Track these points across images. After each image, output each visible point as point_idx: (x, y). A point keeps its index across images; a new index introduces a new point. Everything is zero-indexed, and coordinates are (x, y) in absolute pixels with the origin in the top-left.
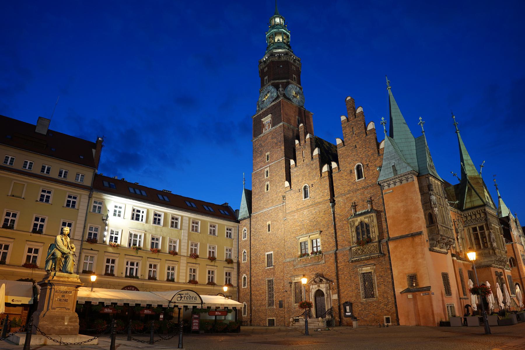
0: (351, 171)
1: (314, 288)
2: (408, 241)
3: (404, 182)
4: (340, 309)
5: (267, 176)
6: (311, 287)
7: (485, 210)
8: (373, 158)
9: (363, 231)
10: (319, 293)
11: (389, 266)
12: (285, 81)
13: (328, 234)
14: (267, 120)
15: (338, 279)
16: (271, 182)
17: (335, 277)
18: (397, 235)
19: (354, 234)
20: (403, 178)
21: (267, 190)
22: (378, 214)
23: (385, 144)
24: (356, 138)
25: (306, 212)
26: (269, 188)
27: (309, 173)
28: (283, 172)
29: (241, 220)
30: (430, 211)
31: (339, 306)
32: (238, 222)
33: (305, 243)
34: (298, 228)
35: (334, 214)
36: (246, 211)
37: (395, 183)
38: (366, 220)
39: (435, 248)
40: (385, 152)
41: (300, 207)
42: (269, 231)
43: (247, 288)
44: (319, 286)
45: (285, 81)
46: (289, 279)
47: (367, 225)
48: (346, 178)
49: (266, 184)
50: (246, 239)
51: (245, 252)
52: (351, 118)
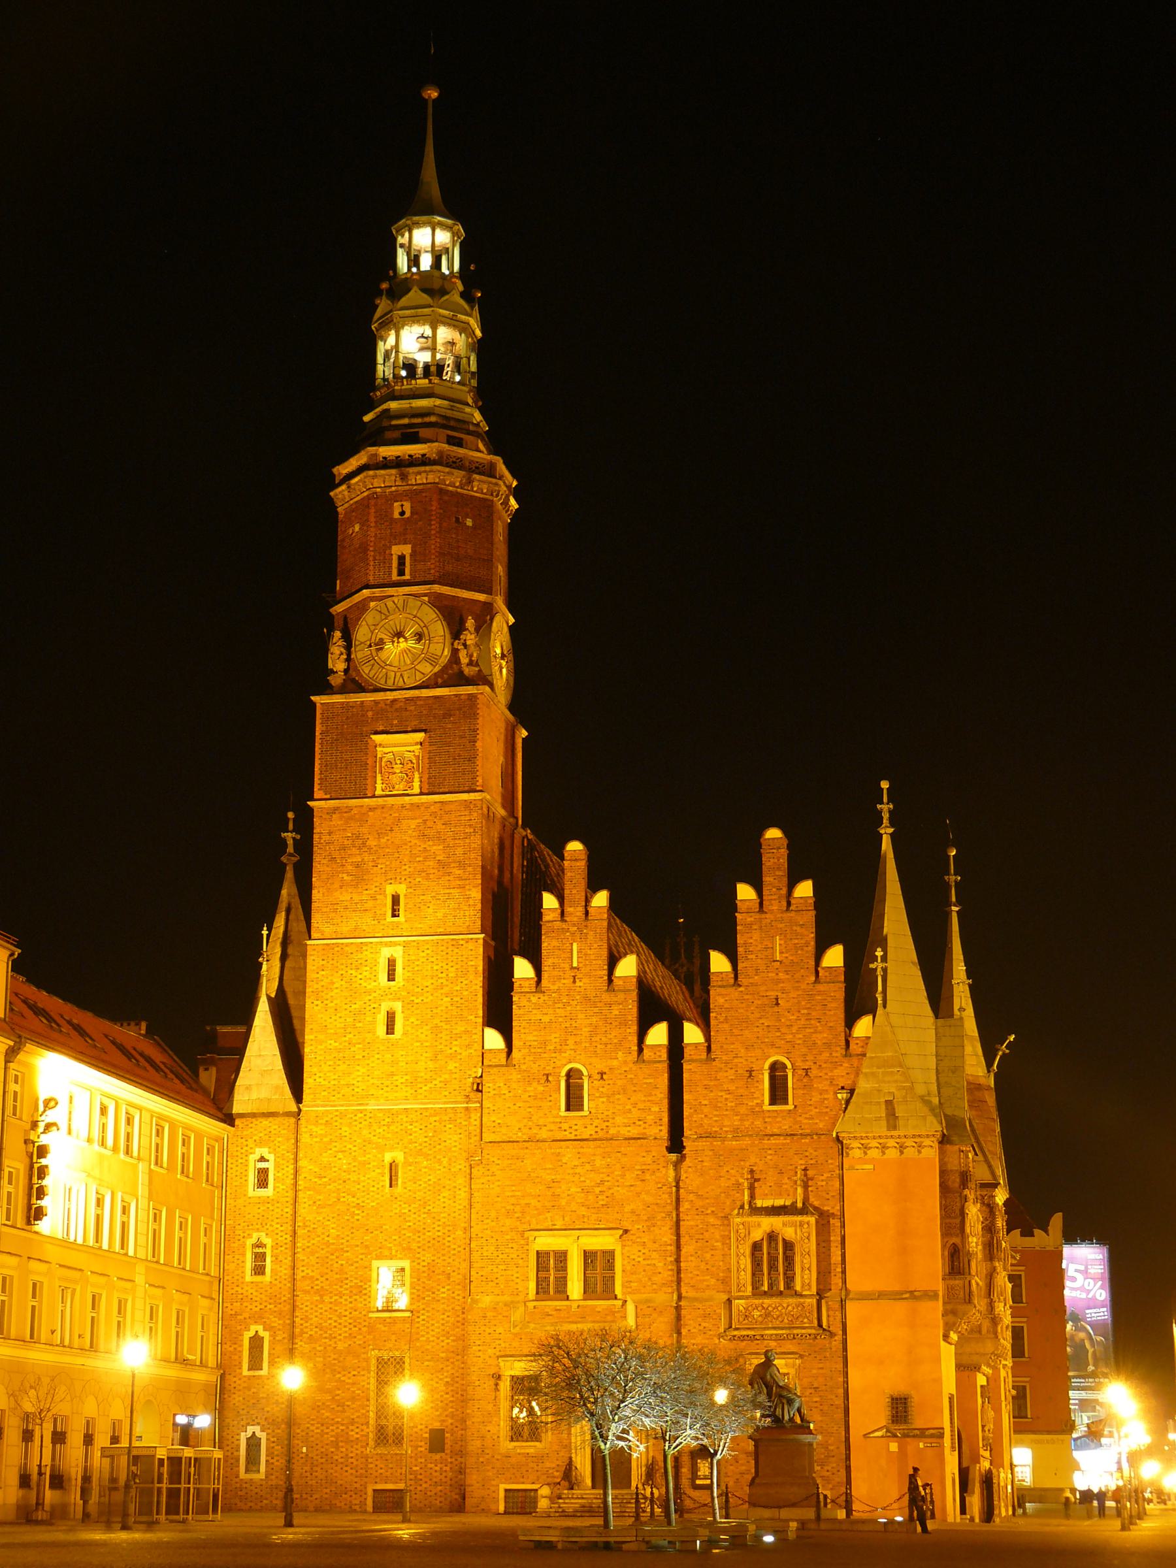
0: (750, 1071)
2: (900, 1309)
3: (910, 1152)
5: (391, 977)
8: (826, 1055)
11: (840, 1366)
12: (482, 597)
13: (650, 1245)
16: (408, 1005)
18: (868, 1286)
19: (746, 1262)
20: (909, 1142)
21: (390, 1030)
22: (824, 1219)
25: (569, 1154)
28: (474, 987)
29: (242, 1116)
30: (956, 1240)
32: (229, 1119)
33: (562, 1257)
34: (533, 1202)
35: (678, 1187)
36: (277, 1087)
37: (884, 1148)
38: (789, 1233)
41: (544, 1134)
45: (482, 597)
46: (492, 1362)
47: (789, 1246)
48: (732, 1087)
49: (385, 1007)
50: (269, 1192)
51: (259, 1245)
52: (774, 904)
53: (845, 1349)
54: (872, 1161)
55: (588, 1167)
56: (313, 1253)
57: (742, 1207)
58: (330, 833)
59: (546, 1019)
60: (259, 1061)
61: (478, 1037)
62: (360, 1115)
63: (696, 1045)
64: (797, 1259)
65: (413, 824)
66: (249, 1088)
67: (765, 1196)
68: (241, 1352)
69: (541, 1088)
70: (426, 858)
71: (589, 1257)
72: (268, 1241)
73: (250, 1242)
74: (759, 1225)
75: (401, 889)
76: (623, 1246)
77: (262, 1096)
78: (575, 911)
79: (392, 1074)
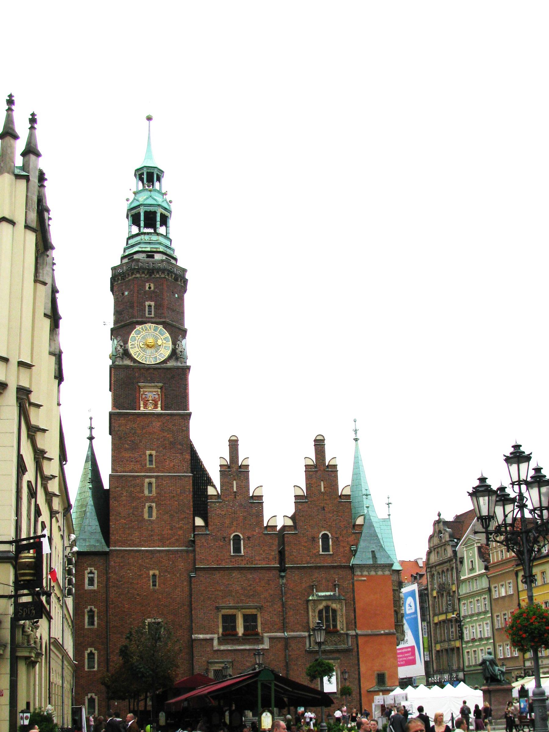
0: (314, 539)
8: (345, 532)
9: (327, 618)
21: (150, 515)
24: (325, 497)
27: (245, 518)
28: (188, 498)
34: (220, 594)
38: (334, 606)
42: (154, 585)
43: (98, 671)
47: (334, 611)
49: (147, 505)
51: (91, 611)
53: (358, 655)
54: (366, 576)
55: (244, 578)
56: (116, 616)
57: (313, 596)
58: (119, 427)
59: (223, 513)
60: (89, 528)
61: (191, 521)
62: (137, 554)
68: (84, 660)
69: (222, 543)
70: (164, 439)
71: (246, 618)
72: (96, 610)
74: (321, 603)
75: (154, 453)
76: (261, 613)
77: (92, 544)
79: (152, 536)
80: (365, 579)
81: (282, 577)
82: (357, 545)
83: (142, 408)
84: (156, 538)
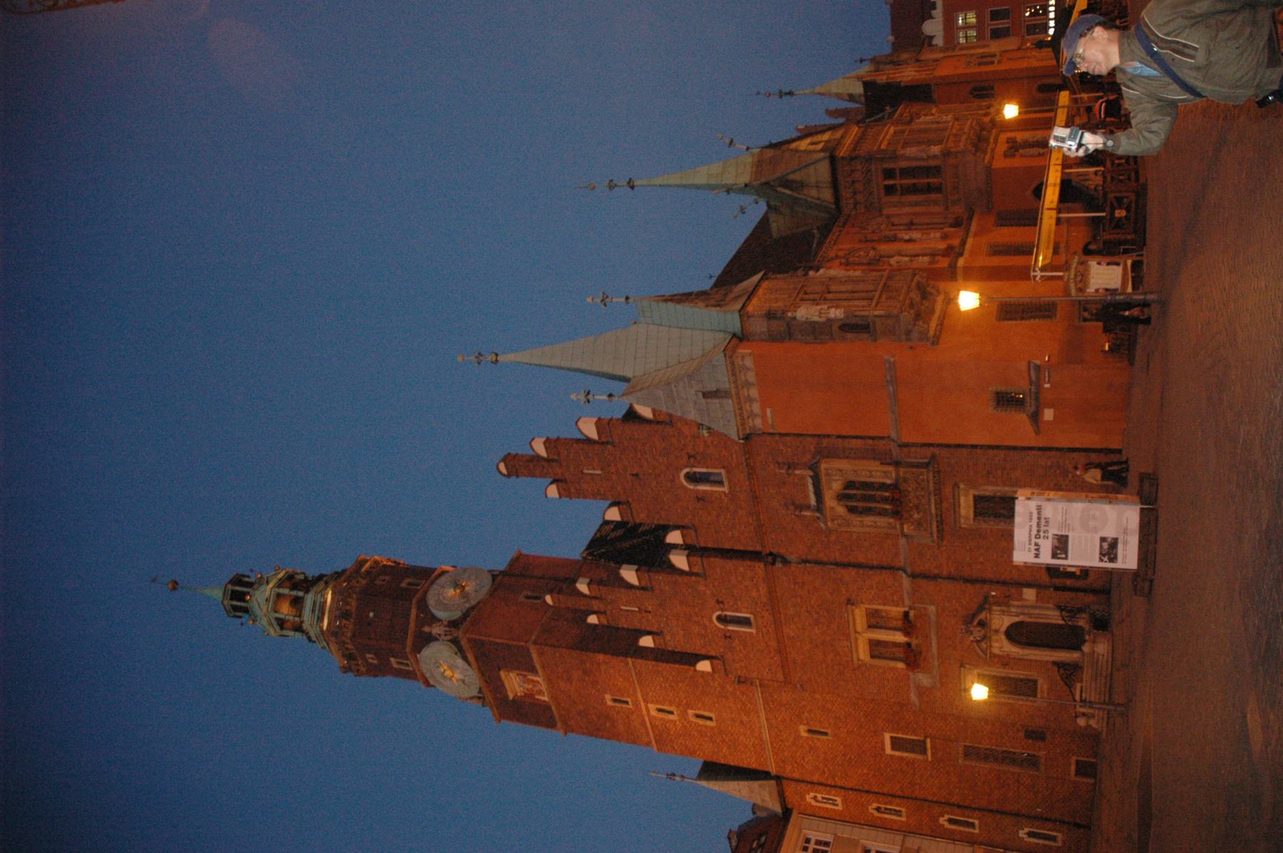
0: (701, 498)
1: (1002, 646)
4: (1064, 589)
5: (672, 713)
6: (996, 651)
7: (843, 158)
10: (1016, 634)
11: (965, 451)
14: (514, 683)
15: (984, 581)
16: (689, 706)
17: (978, 586)
19: (869, 520)
21: (710, 719)
23: (645, 405)
26: (706, 714)
28: (669, 670)
30: (835, 328)
31: (1057, 589)
32: (787, 813)
33: (875, 645)
35: (806, 561)
37: (750, 400)
38: (837, 486)
39: (931, 333)
40: (664, 409)
41: (773, 644)
42: (826, 734)
44: (997, 631)
47: (850, 485)
53: (948, 446)
54: (763, 409)
59: (681, 632)
63: (683, 536)
64: (862, 479)
65: (562, 685)
66: (763, 800)
67: (807, 496)
72: (875, 805)
73: (876, 814)
74: (832, 508)
78: (596, 605)
79: (742, 722)
80: (768, 410)
81: (786, 562)
82: (700, 425)
83: (546, 699)
84: (745, 718)
